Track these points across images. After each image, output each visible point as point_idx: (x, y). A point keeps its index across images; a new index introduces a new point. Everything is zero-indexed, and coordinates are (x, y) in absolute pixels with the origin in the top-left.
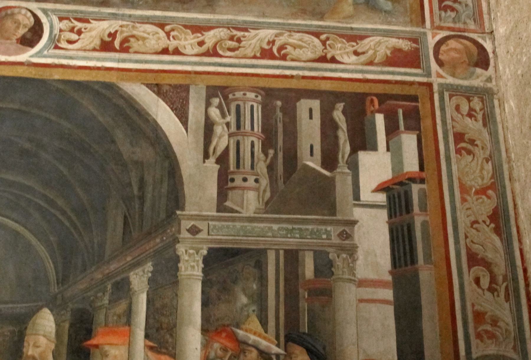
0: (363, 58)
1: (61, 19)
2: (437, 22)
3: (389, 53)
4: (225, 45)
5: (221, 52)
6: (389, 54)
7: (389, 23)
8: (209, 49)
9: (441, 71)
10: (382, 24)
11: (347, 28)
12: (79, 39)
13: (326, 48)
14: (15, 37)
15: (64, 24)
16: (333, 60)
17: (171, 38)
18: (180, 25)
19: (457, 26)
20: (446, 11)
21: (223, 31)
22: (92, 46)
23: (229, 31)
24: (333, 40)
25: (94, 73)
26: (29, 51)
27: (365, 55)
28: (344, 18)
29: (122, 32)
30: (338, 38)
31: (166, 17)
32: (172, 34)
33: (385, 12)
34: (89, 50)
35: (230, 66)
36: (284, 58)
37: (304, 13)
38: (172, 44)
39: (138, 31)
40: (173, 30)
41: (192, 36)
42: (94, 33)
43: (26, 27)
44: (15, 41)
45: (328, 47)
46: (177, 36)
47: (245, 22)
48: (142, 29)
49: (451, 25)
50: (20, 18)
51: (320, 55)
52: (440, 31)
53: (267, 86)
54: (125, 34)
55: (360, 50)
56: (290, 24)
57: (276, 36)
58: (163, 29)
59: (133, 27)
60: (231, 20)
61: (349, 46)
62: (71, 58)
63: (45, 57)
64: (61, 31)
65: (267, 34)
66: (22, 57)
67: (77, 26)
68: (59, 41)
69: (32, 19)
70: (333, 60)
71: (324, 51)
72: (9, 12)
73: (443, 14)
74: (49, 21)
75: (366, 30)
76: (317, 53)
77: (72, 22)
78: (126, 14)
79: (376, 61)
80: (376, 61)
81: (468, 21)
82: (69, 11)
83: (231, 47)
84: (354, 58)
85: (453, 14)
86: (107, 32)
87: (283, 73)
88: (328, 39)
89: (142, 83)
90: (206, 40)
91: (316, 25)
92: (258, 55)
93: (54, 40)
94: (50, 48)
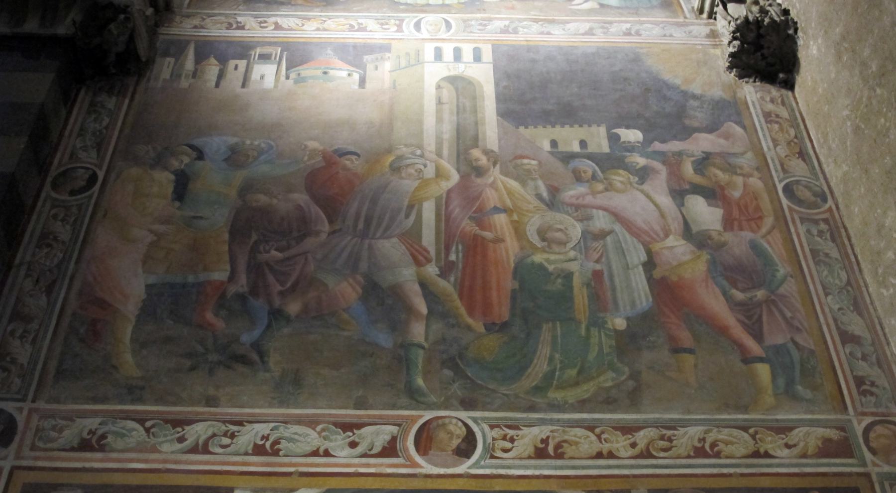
0: (795, 451)
1: (492, 427)
2: (860, 409)
3: (820, 443)
4: (657, 445)
5: (655, 453)
6: (820, 445)
7: (812, 412)
8: (642, 451)
9: (875, 459)
10: (806, 413)
11: (772, 420)
12: (513, 447)
13: (757, 443)
14: (450, 449)
15: (496, 433)
16: (767, 455)
17: (603, 442)
18: (609, 427)
19: (880, 410)
20: (865, 396)
21: (652, 431)
22: (526, 454)
23: (658, 430)
24: (762, 434)
25: (534, 481)
26: (465, 462)
27: (797, 447)
28: (767, 410)
29: (554, 438)
30: (765, 430)
32: (603, 436)
33: (807, 400)
34: (524, 458)
35: (666, 467)
36: (718, 455)
37: (726, 406)
38: (605, 447)
39: (570, 436)
40: (603, 432)
41: (623, 438)
42: (526, 440)
43: (459, 437)
44: (450, 453)
45: (759, 442)
46: (608, 438)
47: (672, 420)
48: (572, 433)
49: (874, 410)
50: (452, 428)
51: (753, 450)
52: (865, 417)
53: (708, 487)
54: (557, 440)
55: (790, 443)
56: (716, 420)
57: (705, 433)
58: (593, 432)
59: (564, 431)
60: (658, 419)
61: (779, 439)
62: (509, 467)
63: (482, 467)
64: (494, 439)
65: (695, 431)
66: (461, 469)
67: (508, 434)
68: (493, 450)
69: (464, 429)
70: (767, 455)
71: (756, 445)
73: (864, 399)
74: (480, 429)
75: (792, 420)
76: (750, 448)
77: (503, 430)
78: (554, 419)
79: (810, 453)
80: (810, 453)
81: (889, 405)
82: (501, 419)
83: (663, 447)
84: (786, 452)
85: (873, 399)
86: (539, 439)
87: (720, 472)
88: (756, 433)
89: (583, 491)
90: (638, 441)
91: (741, 419)
92: (692, 454)
93: (489, 450)
94: (486, 459)
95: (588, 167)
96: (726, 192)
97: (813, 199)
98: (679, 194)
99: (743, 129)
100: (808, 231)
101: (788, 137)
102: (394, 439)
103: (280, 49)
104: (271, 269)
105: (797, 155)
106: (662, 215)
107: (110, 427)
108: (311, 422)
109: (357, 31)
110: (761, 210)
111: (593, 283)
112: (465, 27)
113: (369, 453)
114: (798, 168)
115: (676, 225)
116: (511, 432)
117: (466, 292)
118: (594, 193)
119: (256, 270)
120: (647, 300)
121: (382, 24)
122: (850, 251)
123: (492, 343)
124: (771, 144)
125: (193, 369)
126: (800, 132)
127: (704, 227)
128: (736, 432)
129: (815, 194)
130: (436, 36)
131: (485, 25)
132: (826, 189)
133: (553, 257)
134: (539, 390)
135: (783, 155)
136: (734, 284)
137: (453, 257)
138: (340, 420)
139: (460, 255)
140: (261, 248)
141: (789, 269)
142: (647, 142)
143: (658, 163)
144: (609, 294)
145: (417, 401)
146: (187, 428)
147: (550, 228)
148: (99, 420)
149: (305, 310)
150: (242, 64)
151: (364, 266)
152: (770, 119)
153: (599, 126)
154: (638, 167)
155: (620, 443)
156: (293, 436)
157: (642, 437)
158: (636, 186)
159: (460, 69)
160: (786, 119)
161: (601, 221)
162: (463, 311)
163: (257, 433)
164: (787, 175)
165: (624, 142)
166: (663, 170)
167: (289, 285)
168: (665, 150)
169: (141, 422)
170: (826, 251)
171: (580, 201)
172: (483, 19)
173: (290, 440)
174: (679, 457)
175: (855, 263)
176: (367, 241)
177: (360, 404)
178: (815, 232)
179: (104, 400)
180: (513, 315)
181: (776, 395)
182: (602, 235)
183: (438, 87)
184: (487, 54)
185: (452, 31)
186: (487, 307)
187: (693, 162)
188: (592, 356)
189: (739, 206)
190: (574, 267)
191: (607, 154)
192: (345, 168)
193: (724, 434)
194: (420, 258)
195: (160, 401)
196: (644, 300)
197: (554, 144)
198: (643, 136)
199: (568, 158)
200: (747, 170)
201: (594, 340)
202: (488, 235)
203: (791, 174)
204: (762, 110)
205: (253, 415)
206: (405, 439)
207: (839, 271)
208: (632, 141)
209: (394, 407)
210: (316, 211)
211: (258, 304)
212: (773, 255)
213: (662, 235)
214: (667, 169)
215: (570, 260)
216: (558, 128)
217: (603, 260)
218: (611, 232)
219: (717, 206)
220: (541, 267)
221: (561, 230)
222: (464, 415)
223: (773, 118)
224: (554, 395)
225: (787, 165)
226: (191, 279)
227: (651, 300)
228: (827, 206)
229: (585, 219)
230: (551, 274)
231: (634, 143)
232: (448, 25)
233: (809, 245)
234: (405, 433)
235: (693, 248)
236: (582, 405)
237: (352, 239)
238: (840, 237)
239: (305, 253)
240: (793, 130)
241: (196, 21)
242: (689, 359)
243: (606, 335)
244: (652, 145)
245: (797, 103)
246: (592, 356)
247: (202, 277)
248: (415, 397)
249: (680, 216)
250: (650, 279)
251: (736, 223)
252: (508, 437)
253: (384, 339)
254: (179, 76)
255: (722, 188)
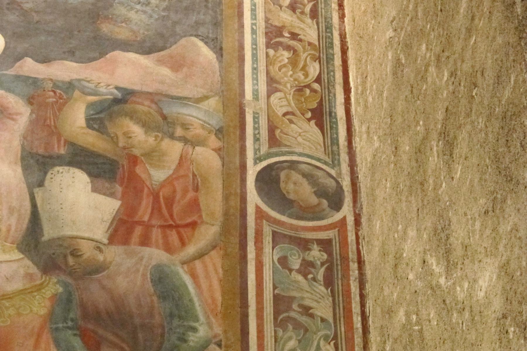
96: (138, 170)
97: (314, 200)
99: (215, 53)
100: (283, 261)
101: (302, 77)
105: (309, 115)
110: (199, 210)
122: (356, 308)
124: (263, 88)
126: (331, 72)
127: (68, 232)
129: (321, 193)
132: (346, 183)
135: (280, 112)
141: (218, 330)
143: (17, 99)
152: (278, 39)
160: (310, 44)
164: (274, 150)
168: (41, 77)
170: (307, 303)
175: (360, 330)
178: (296, 263)
187: (90, 106)
189: (156, 197)
198: (6, 43)
200: (197, 131)
203: (284, 149)
204: (267, 20)
207: (322, 343)
212: (195, 299)
214: (32, 112)
219: (112, 195)
223: (286, 39)
225: (282, 132)
228: (338, 216)
233: (275, 288)
235: (34, 270)
238: (346, 276)
240: (317, 65)
244: (18, 64)
245: (342, 17)
249: (27, 204)
251: (138, 231)
255: (134, 160)
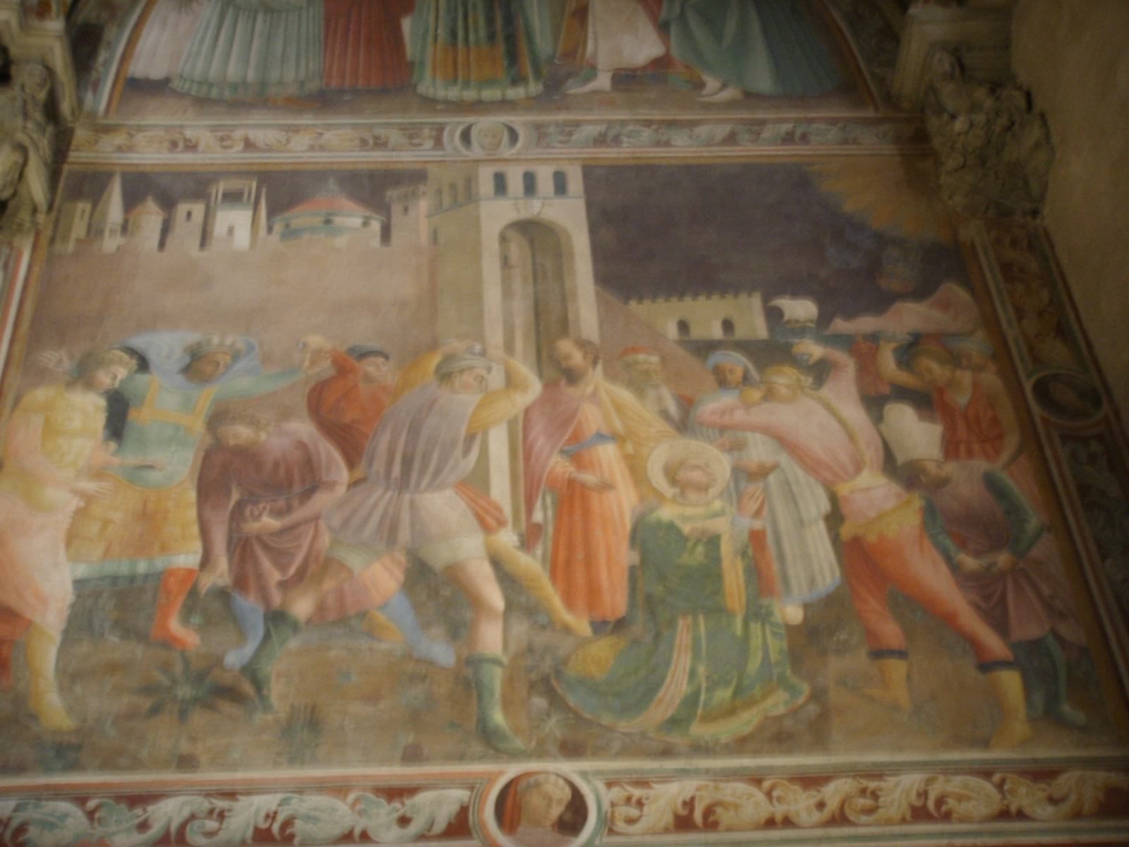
1: (610, 785)
5: (852, 817)
14: (549, 823)
15: (616, 793)
16: (1021, 815)
22: (662, 824)
23: (856, 782)
31: (759, 768)
36: (947, 817)
37: (958, 741)
38: (779, 811)
47: (875, 764)
50: (549, 788)
59: (716, 788)
70: (1021, 815)
72: (532, 780)
77: (626, 790)
84: (1050, 810)
88: (1003, 781)
95: (736, 362)
98: (874, 403)
102: (464, 811)
103: (254, 185)
104: (266, 547)
106: (851, 437)
107: (31, 813)
108: (339, 789)
109: (372, 149)
111: (750, 552)
112: (539, 138)
113: (427, 833)
114: (1056, 352)
115: (872, 454)
116: (637, 792)
117: (560, 569)
118: (748, 406)
119: (242, 548)
120: (832, 572)
121: (411, 137)
123: (603, 650)
125: (155, 710)
128: (974, 781)
130: (495, 154)
131: (570, 134)
133: (689, 511)
134: (675, 723)
136: (962, 544)
137: (538, 516)
138: (382, 784)
139: (550, 513)
140: (247, 512)
142: (824, 319)
144: (775, 567)
145: (497, 750)
146: (150, 808)
147: (682, 464)
148: (11, 804)
149: (321, 609)
150: (198, 209)
151: (404, 535)
153: (750, 295)
154: (812, 361)
155: (800, 803)
156: (312, 813)
157: (833, 792)
158: (810, 392)
159: (535, 208)
161: (759, 451)
162: (557, 602)
163: (258, 810)
165: (789, 322)
166: (849, 367)
167: (292, 570)
169: (81, 800)
171: (726, 419)
172: (566, 123)
173: (308, 818)
174: (889, 822)
176: (407, 497)
177: (412, 755)
179: (20, 769)
180: (632, 604)
181: (1032, 720)
182: (761, 473)
183: (503, 239)
184: (576, 183)
185: (519, 145)
186: (593, 592)
187: (895, 351)
188: (754, 665)
190: (721, 526)
191: (763, 341)
192: (368, 379)
193: (956, 784)
194: (489, 519)
195: (108, 764)
196: (827, 573)
197: (683, 326)
199: (704, 348)
201: (756, 642)
202: (589, 478)
205: (252, 781)
206: (481, 810)
208: (802, 320)
209: (461, 757)
210: (327, 451)
211: (249, 605)
213: (851, 469)
215: (716, 515)
216: (688, 301)
217: (766, 511)
218: (775, 467)
219: (932, 419)
220: (671, 527)
221: (698, 467)
222: (568, 767)
224: (699, 730)
226: (142, 567)
227: (838, 574)
229: (736, 447)
230: (687, 539)
231: (804, 322)
232: (514, 136)
234: (481, 798)
236: (740, 745)
237: (383, 495)
239: (316, 518)
241: (120, 139)
242: (897, 668)
243: (774, 634)
246: (754, 665)
247: (160, 563)
248: (491, 742)
250: (835, 539)
251: (963, 447)
252: (634, 800)
253: (442, 653)
254: (100, 233)
255: (941, 391)
